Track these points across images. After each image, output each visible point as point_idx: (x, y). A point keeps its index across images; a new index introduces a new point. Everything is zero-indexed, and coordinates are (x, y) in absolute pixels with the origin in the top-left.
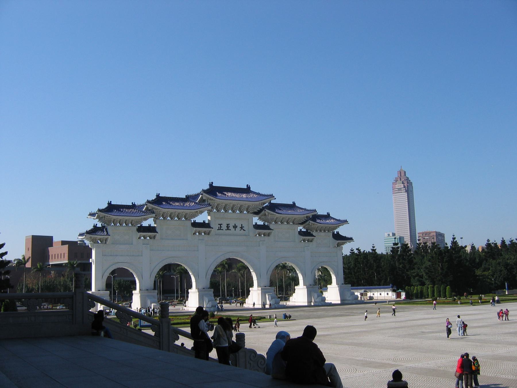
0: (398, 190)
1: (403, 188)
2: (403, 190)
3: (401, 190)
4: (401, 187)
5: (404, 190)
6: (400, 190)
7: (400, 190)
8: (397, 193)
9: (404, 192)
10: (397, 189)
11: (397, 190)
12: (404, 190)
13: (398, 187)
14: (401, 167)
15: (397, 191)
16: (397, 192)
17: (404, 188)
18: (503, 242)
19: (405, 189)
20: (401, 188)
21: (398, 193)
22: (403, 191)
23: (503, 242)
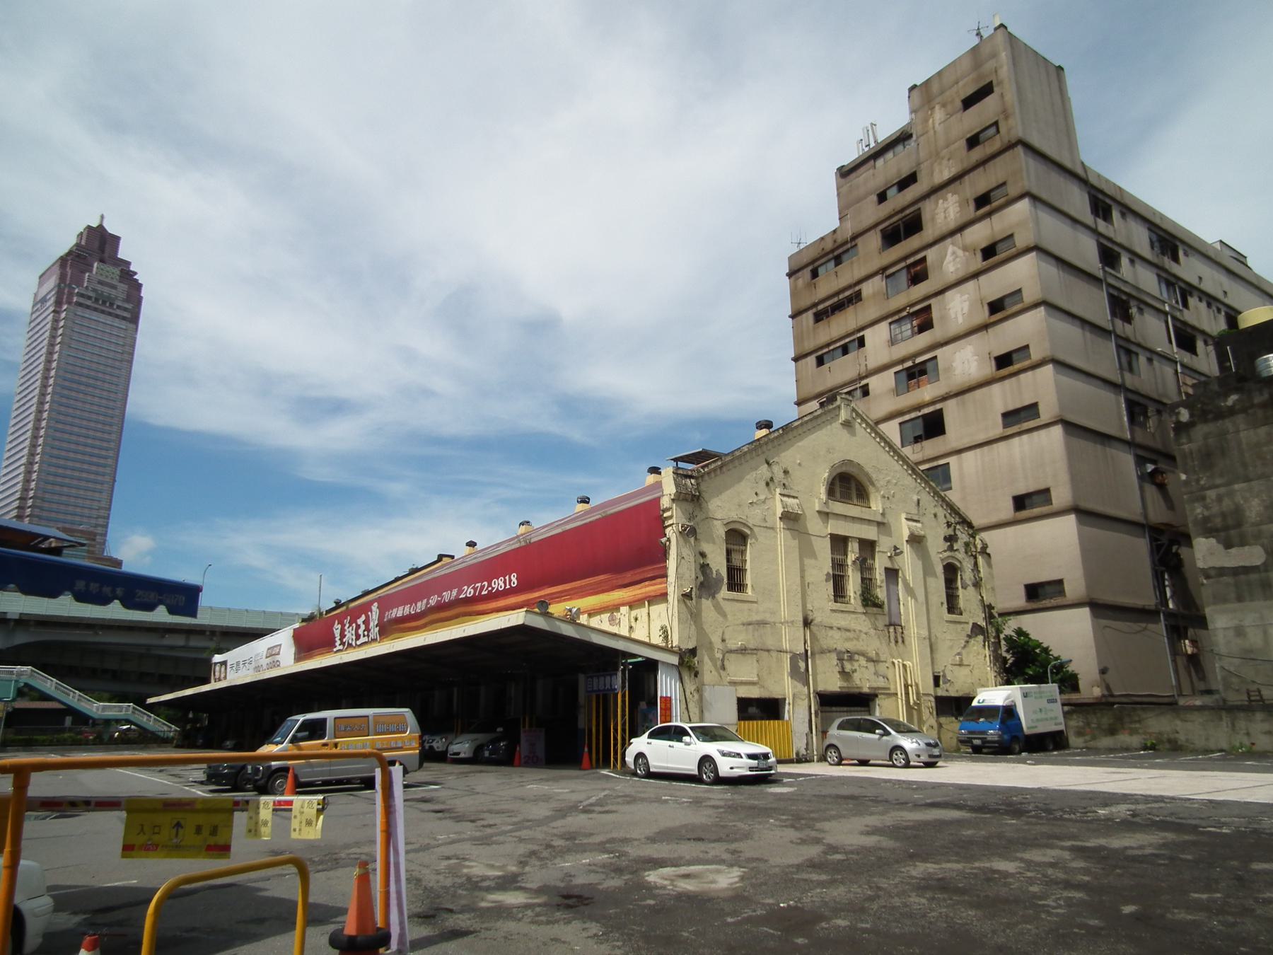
0: (97, 300)
2: (119, 307)
3: (112, 305)
5: (126, 309)
6: (104, 303)
7: (104, 303)
8: (88, 307)
9: (124, 318)
11: (91, 294)
12: (126, 309)
14: (102, 217)
15: (89, 298)
16: (89, 303)
17: (127, 300)
19: (129, 306)
21: (96, 310)
22: (119, 312)
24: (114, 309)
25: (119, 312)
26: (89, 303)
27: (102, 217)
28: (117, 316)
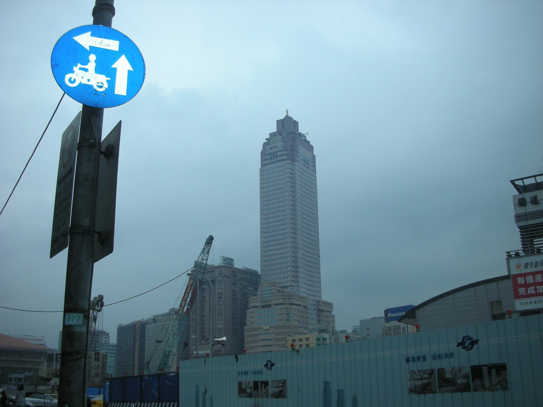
0: (271, 158)
1: (280, 151)
2: (280, 156)
3: (277, 156)
4: (277, 150)
6: (274, 157)
7: (274, 157)
10: (268, 154)
13: (271, 151)
14: (287, 111)
15: (268, 159)
16: (268, 162)
18: (533, 196)
20: (277, 152)
21: (271, 163)
23: (533, 196)
24: (279, 158)
25: (280, 158)
26: (268, 162)
27: (287, 111)
28: (280, 161)
